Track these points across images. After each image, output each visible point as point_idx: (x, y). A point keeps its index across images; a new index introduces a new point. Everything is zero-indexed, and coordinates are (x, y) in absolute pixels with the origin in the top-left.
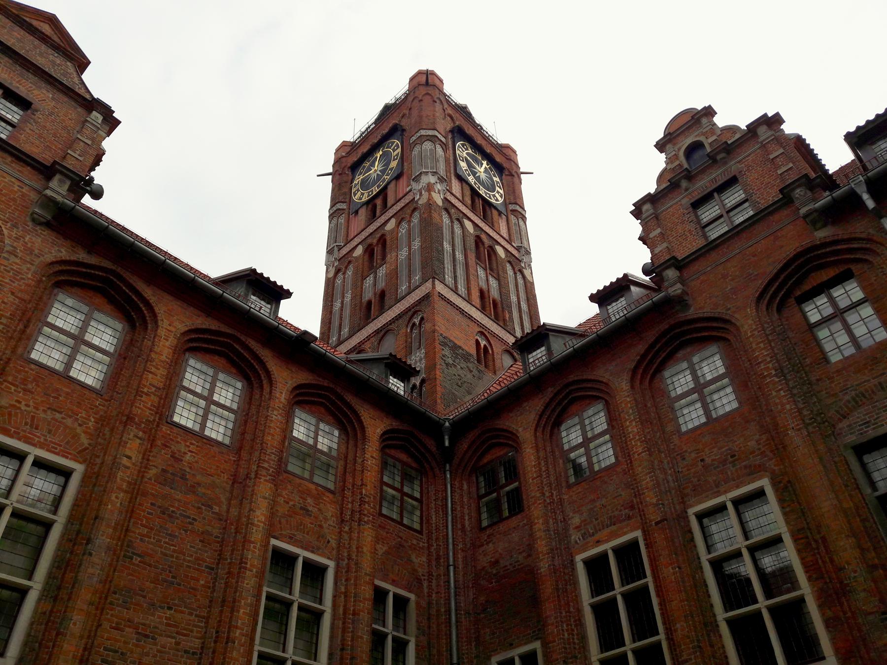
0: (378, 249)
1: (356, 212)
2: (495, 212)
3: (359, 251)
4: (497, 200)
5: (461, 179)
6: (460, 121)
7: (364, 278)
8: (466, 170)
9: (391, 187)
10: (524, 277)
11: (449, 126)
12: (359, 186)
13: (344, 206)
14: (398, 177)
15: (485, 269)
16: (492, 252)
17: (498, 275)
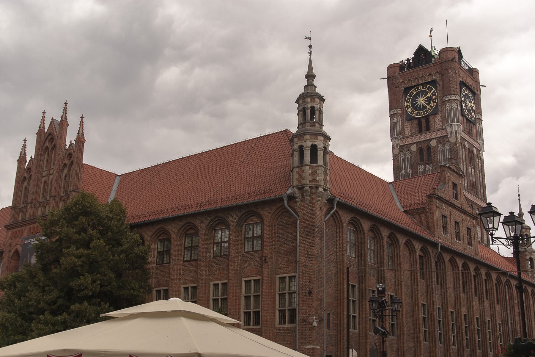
2: (472, 125)
5: (463, 115)
9: (431, 119)
12: (410, 104)
16: (472, 151)
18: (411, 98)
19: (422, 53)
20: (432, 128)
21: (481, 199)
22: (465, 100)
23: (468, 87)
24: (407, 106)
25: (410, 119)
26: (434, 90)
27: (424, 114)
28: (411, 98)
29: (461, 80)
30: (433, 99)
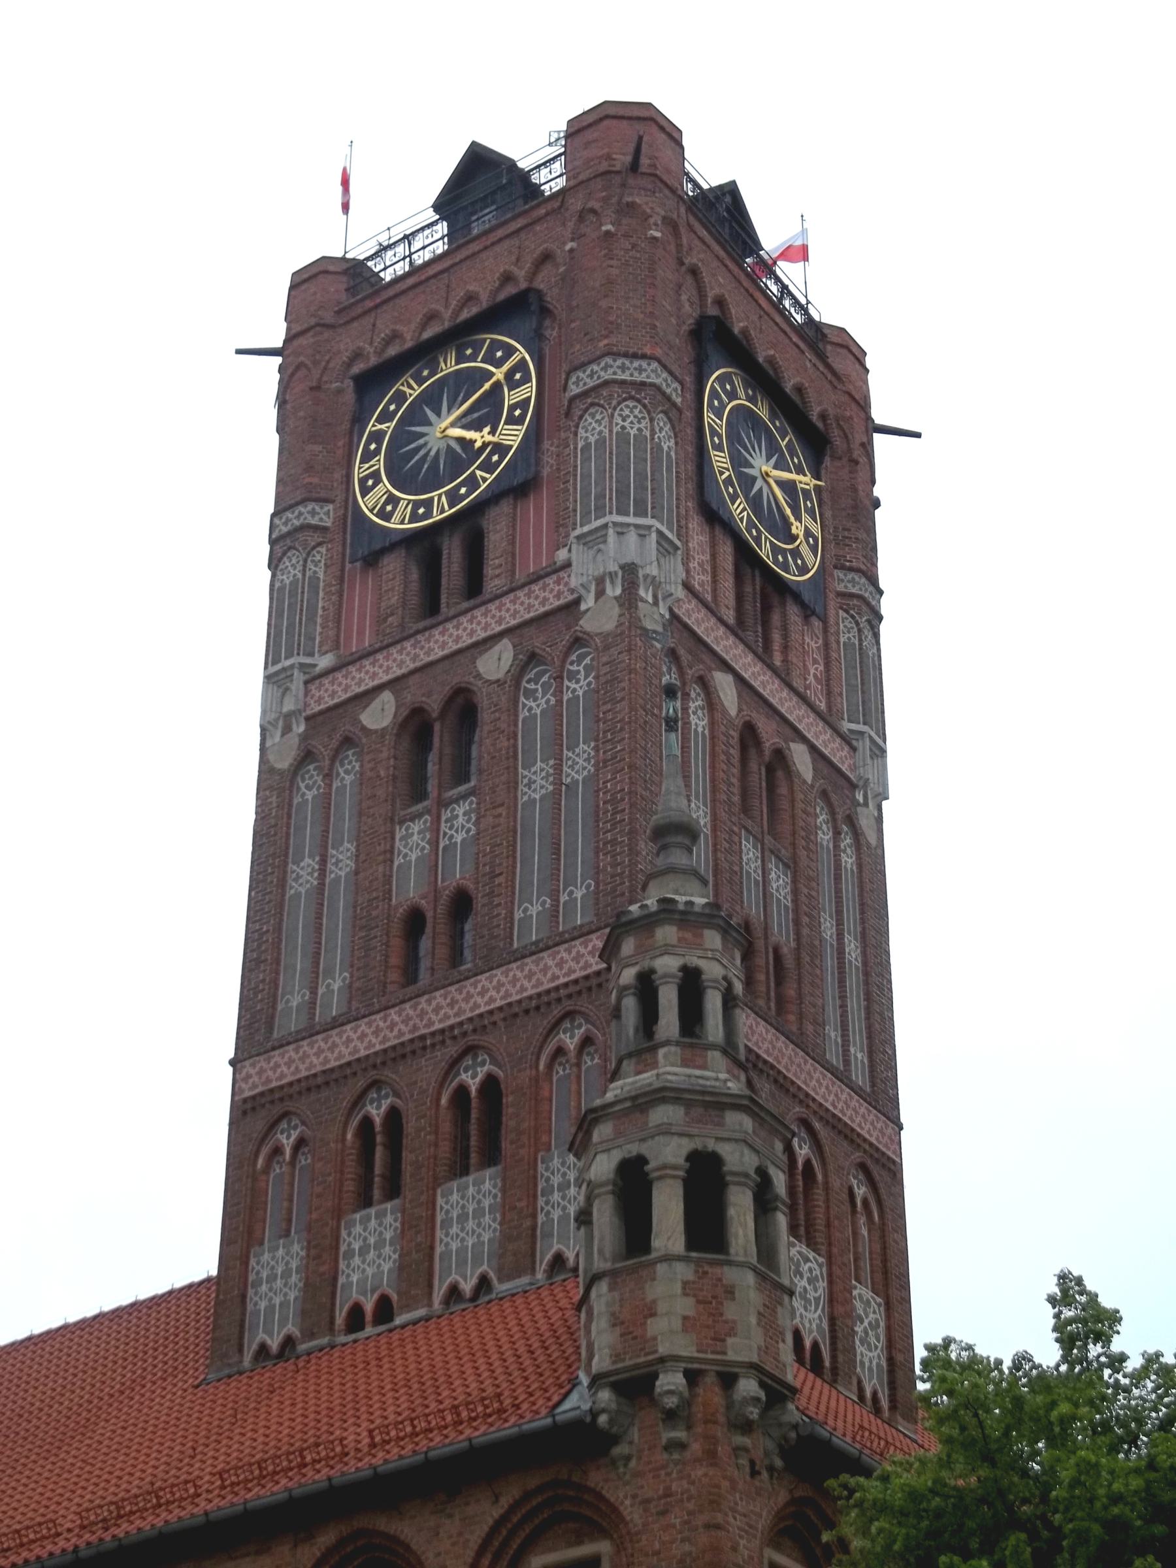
0: (443, 736)
1: (372, 560)
2: (793, 610)
3: (380, 715)
4: (804, 570)
5: (714, 518)
6: (718, 283)
7: (393, 820)
8: (728, 481)
10: (857, 834)
11: (690, 312)
12: (379, 463)
13: (325, 515)
14: (519, 486)
15: (759, 840)
17: (795, 858)
18: (389, 427)
19: (481, 184)
20: (492, 585)
21: (842, 1076)
22: (734, 437)
23: (763, 380)
24: (363, 481)
25: (370, 548)
26: (522, 352)
27: (453, 498)
28: (389, 427)
29: (713, 311)
30: (512, 408)
